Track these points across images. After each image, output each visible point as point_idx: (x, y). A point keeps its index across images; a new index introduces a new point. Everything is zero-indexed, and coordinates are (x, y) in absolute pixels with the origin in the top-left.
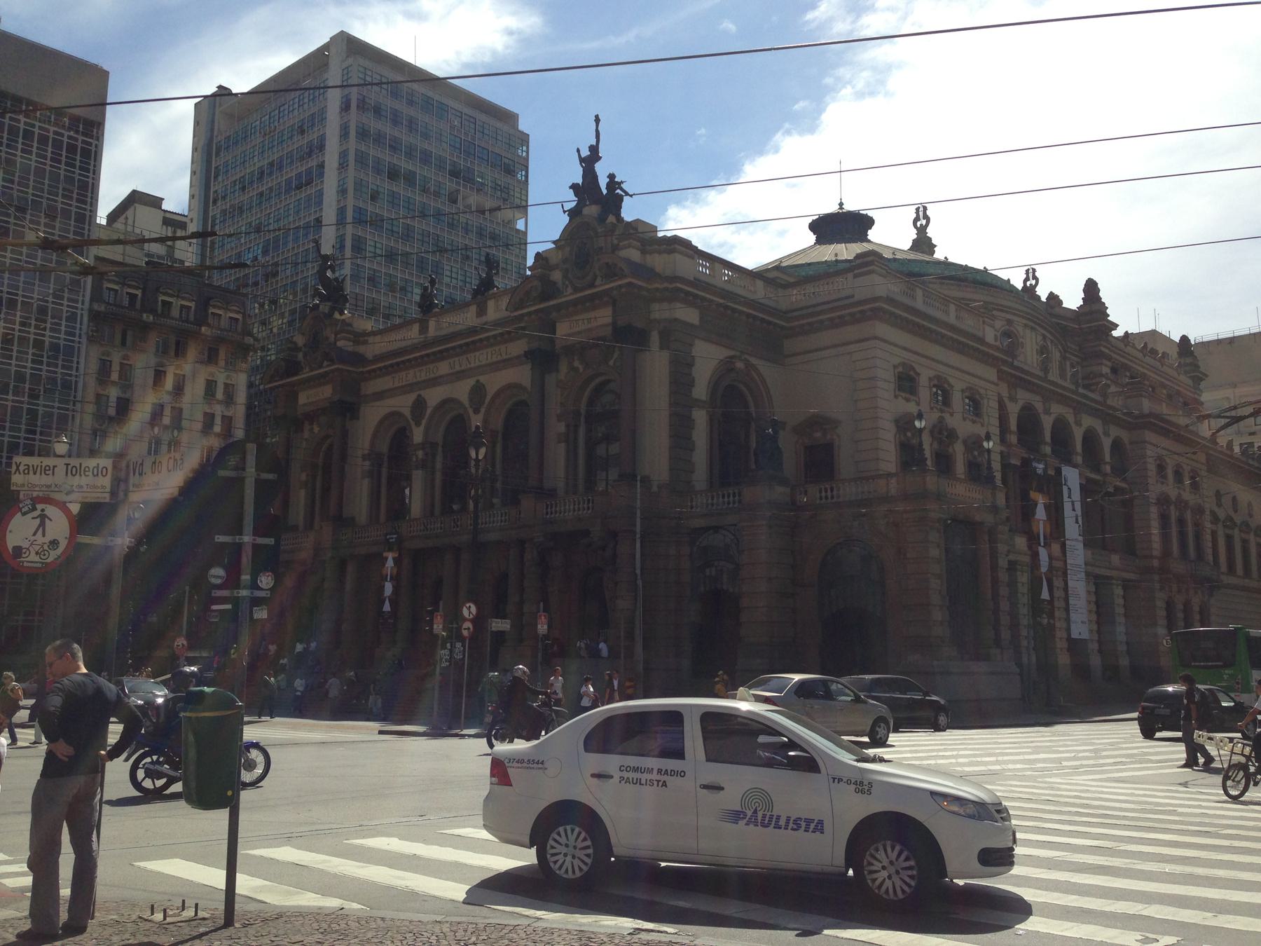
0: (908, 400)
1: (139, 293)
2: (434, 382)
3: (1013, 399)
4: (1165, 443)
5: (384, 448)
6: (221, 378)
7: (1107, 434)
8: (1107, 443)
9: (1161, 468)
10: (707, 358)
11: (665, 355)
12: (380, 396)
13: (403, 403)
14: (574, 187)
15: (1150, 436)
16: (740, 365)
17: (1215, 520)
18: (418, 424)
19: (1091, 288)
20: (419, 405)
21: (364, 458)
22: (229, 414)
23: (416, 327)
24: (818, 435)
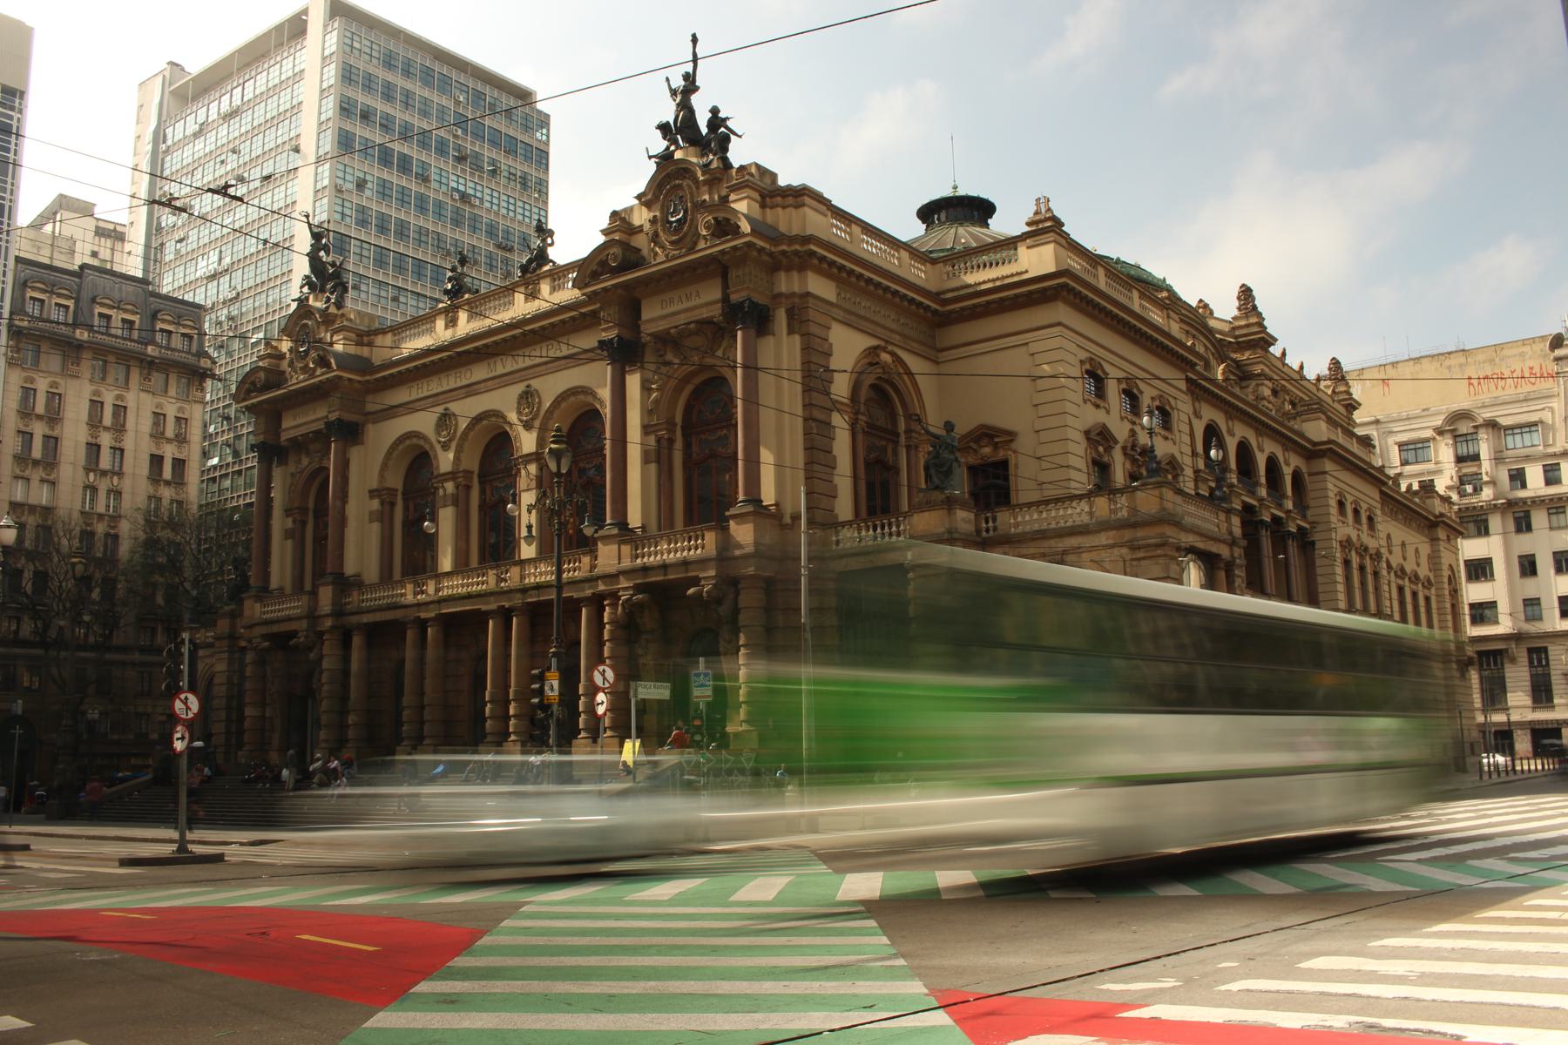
0: (1097, 406)
1: (71, 303)
2: (471, 390)
3: (1197, 415)
4: (1346, 476)
5: (396, 481)
6: (171, 411)
7: (1288, 464)
8: (1287, 471)
9: (1341, 504)
10: (847, 348)
11: (797, 338)
12: (391, 412)
13: (424, 422)
14: (664, 128)
15: (1328, 465)
16: (885, 357)
17: (1389, 566)
18: (445, 446)
19: (1246, 294)
20: (446, 419)
21: (373, 493)
22: (181, 456)
23: (440, 323)
24: (987, 450)
